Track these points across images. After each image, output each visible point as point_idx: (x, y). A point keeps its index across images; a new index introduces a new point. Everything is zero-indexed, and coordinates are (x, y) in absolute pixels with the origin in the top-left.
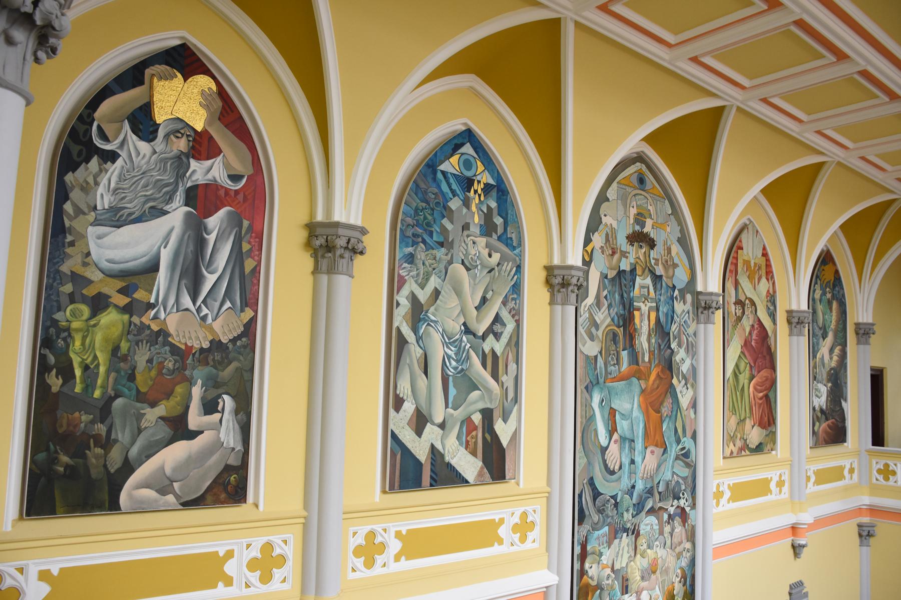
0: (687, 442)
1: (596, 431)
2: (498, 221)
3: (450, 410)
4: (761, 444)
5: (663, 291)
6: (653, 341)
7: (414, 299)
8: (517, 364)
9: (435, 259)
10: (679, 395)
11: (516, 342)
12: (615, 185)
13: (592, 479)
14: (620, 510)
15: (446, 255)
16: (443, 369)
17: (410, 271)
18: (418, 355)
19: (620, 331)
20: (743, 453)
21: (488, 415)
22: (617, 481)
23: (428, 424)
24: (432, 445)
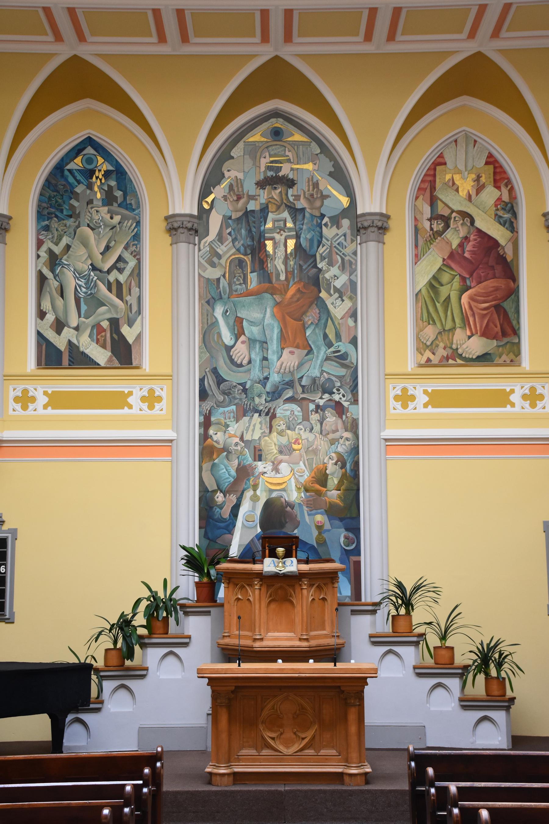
0: (344, 347)
1: (219, 335)
2: (118, 194)
3: (82, 319)
4: (486, 354)
5: (305, 221)
6: (292, 263)
7: (50, 252)
8: (139, 288)
9: (66, 226)
10: (330, 307)
11: (137, 273)
12: (241, 145)
13: (215, 368)
14: (250, 395)
15: (75, 222)
16: (75, 294)
17: (47, 236)
18: (56, 286)
19: (248, 259)
20: (451, 361)
21: (115, 323)
22: (245, 372)
23: (66, 328)
24: (70, 342)
